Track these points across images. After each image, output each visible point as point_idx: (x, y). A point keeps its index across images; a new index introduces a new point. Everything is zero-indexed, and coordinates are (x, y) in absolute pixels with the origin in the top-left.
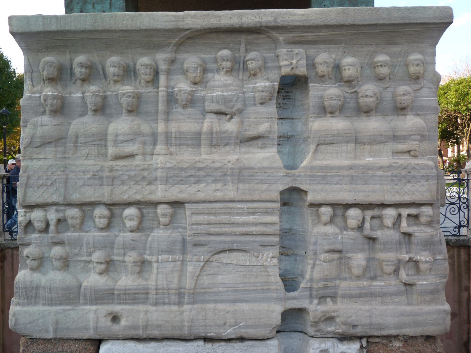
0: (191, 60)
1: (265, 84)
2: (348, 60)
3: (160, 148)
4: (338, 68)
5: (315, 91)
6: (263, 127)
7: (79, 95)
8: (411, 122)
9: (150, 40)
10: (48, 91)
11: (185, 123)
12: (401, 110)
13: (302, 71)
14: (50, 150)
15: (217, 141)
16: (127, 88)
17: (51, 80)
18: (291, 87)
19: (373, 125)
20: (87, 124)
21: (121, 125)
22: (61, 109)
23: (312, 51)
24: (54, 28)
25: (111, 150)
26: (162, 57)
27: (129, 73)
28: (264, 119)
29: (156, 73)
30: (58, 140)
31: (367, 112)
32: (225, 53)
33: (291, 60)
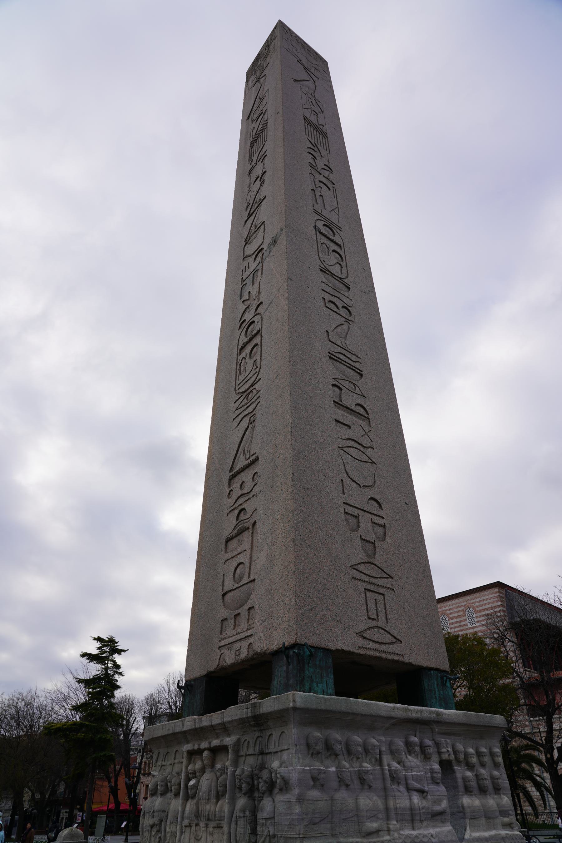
7: (333, 769)
24: (323, 707)
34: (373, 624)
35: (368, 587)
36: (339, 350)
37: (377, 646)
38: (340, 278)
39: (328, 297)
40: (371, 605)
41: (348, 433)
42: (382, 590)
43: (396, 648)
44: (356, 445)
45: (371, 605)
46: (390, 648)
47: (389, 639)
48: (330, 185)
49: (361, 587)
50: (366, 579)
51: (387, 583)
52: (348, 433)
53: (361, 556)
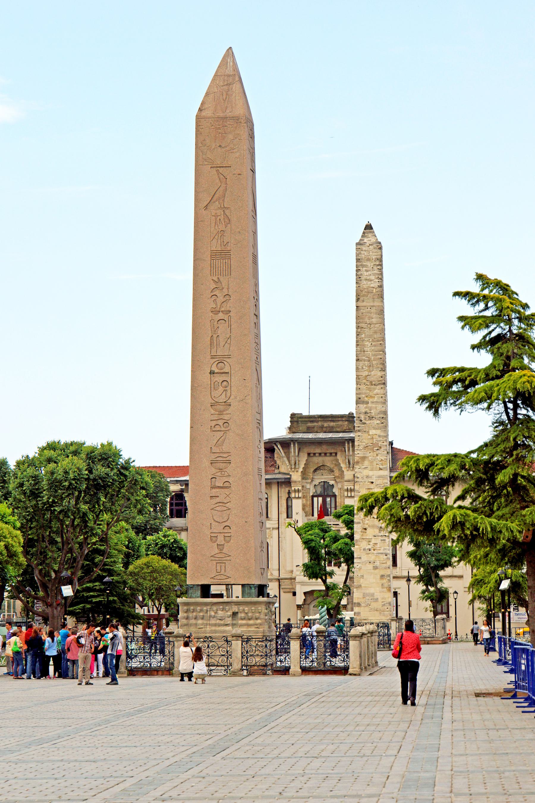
0: (215, 608)
1: (229, 613)
2: (246, 609)
3: (208, 626)
4: (244, 610)
5: (240, 615)
6: (229, 622)
8: (259, 621)
9: (206, 604)
10: (185, 615)
11: (213, 621)
12: (257, 619)
13: (237, 611)
14: (185, 627)
15: (220, 625)
16: (201, 614)
17: (186, 612)
18: (235, 614)
19: (251, 622)
20: (193, 621)
21: (200, 622)
22: (187, 618)
23: (239, 606)
25: (198, 627)
26: (209, 607)
27: (201, 611)
28: (229, 621)
29: (207, 611)
30: (186, 625)
31: (250, 619)
32: (221, 607)
33: (235, 609)
34: (218, 574)
35: (218, 562)
36: (218, 455)
37: (219, 581)
38: (225, 402)
39: (214, 423)
40: (218, 568)
41: (218, 500)
42: (224, 562)
43: (228, 580)
44: (221, 504)
45: (218, 568)
46: (225, 580)
47: (226, 577)
48: (226, 317)
49: (214, 562)
50: (217, 559)
51: (228, 558)
52: (218, 500)
53: (217, 551)
